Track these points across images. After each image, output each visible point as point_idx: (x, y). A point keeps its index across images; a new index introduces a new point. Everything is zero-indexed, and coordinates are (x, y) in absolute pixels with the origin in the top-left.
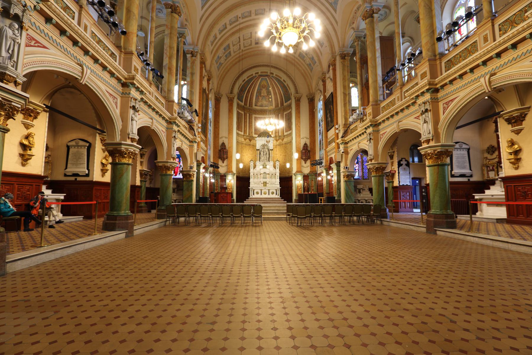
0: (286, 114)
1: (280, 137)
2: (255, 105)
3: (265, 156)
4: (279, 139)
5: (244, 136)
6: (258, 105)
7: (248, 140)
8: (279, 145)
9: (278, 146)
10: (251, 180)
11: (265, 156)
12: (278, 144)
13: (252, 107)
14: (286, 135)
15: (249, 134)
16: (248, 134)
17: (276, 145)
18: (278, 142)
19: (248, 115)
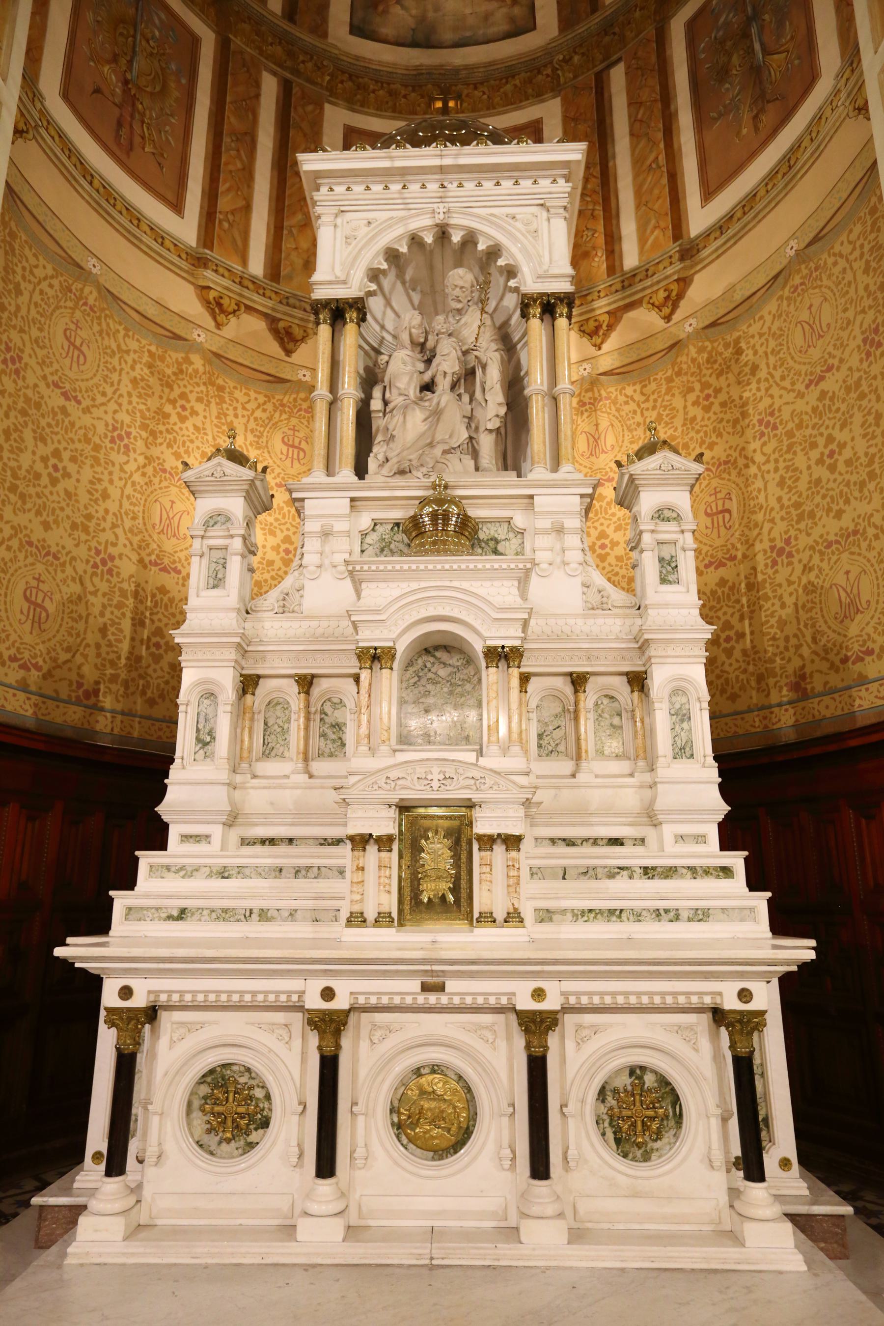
0: (691, 26)
1: (629, 280)
2: (358, 29)
3: (443, 395)
4: (616, 315)
5: (200, 262)
6: (386, 31)
7: (259, 325)
8: (618, 373)
9: (611, 390)
10: (175, 773)
11: (443, 395)
12: (607, 362)
13: (320, 29)
14: (720, 228)
15: (274, 271)
16: (257, 266)
17: (591, 384)
18: (612, 343)
19: (270, 86)
